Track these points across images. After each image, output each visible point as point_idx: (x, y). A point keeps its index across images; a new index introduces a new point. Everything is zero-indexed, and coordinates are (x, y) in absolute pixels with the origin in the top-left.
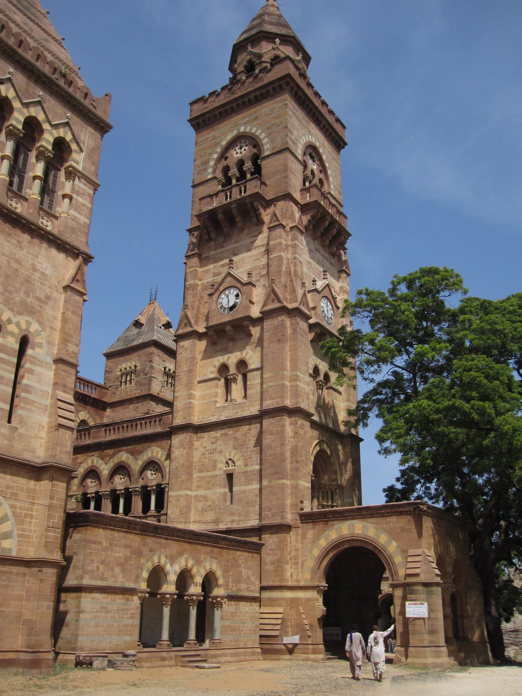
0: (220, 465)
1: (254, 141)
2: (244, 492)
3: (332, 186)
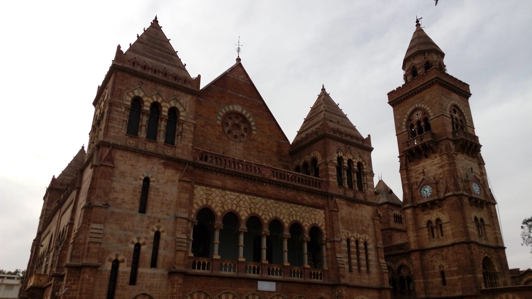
0: (437, 268)
1: (425, 112)
2: (451, 280)
3: (467, 121)
